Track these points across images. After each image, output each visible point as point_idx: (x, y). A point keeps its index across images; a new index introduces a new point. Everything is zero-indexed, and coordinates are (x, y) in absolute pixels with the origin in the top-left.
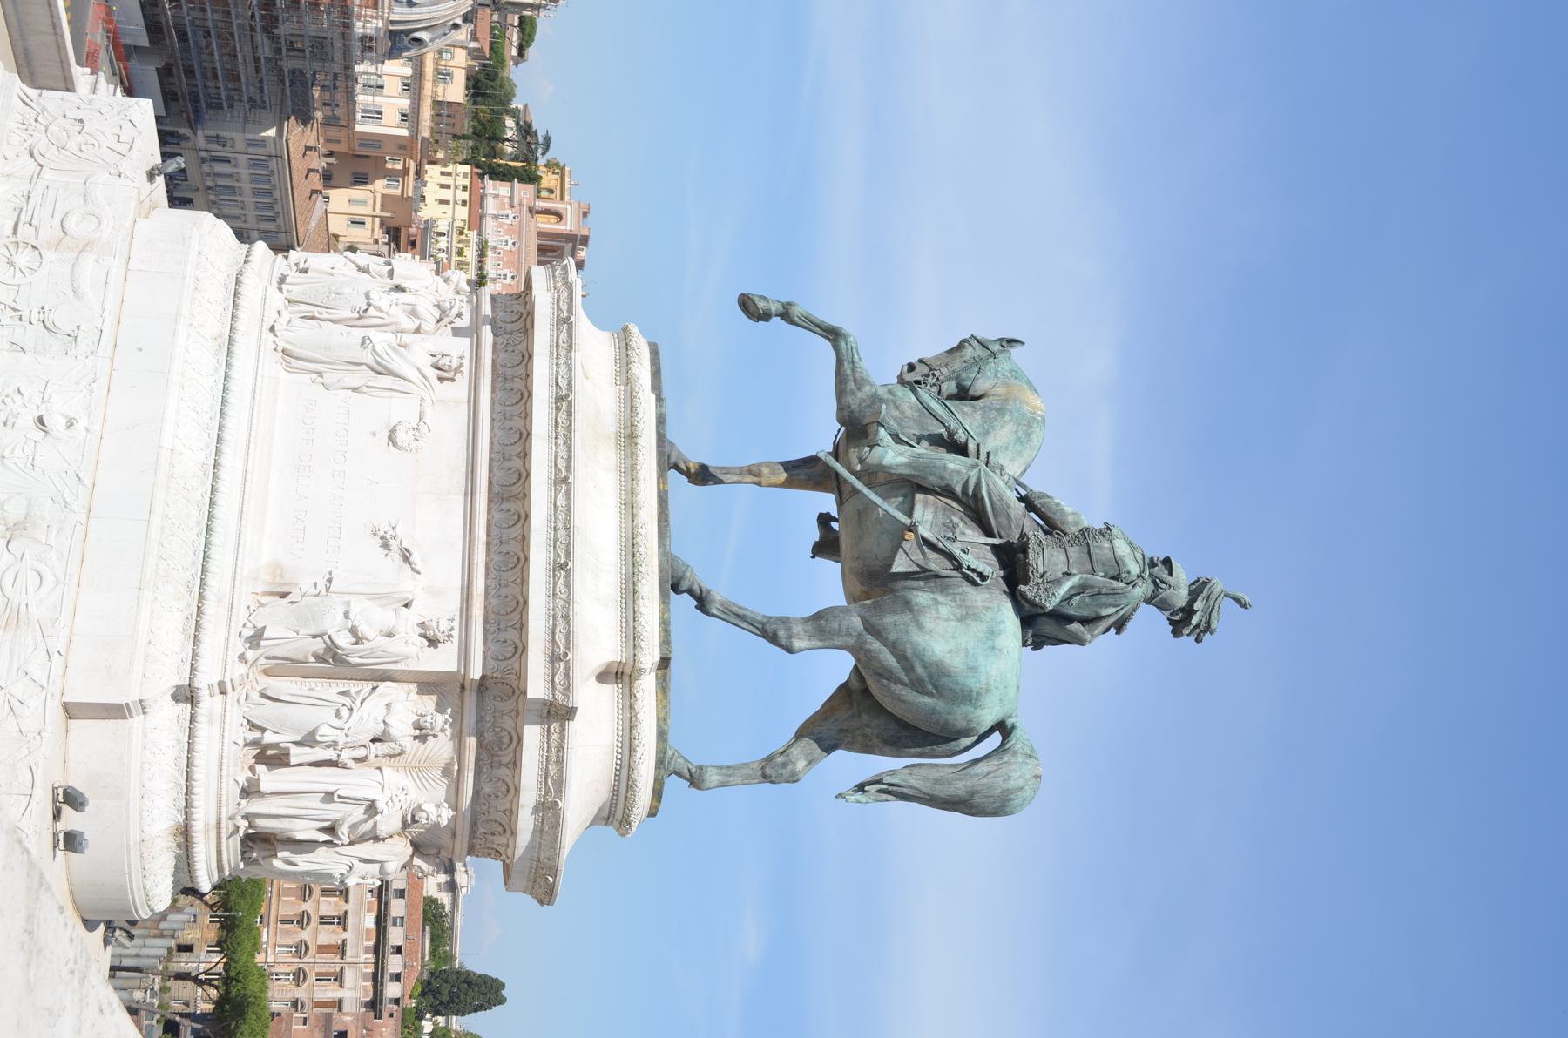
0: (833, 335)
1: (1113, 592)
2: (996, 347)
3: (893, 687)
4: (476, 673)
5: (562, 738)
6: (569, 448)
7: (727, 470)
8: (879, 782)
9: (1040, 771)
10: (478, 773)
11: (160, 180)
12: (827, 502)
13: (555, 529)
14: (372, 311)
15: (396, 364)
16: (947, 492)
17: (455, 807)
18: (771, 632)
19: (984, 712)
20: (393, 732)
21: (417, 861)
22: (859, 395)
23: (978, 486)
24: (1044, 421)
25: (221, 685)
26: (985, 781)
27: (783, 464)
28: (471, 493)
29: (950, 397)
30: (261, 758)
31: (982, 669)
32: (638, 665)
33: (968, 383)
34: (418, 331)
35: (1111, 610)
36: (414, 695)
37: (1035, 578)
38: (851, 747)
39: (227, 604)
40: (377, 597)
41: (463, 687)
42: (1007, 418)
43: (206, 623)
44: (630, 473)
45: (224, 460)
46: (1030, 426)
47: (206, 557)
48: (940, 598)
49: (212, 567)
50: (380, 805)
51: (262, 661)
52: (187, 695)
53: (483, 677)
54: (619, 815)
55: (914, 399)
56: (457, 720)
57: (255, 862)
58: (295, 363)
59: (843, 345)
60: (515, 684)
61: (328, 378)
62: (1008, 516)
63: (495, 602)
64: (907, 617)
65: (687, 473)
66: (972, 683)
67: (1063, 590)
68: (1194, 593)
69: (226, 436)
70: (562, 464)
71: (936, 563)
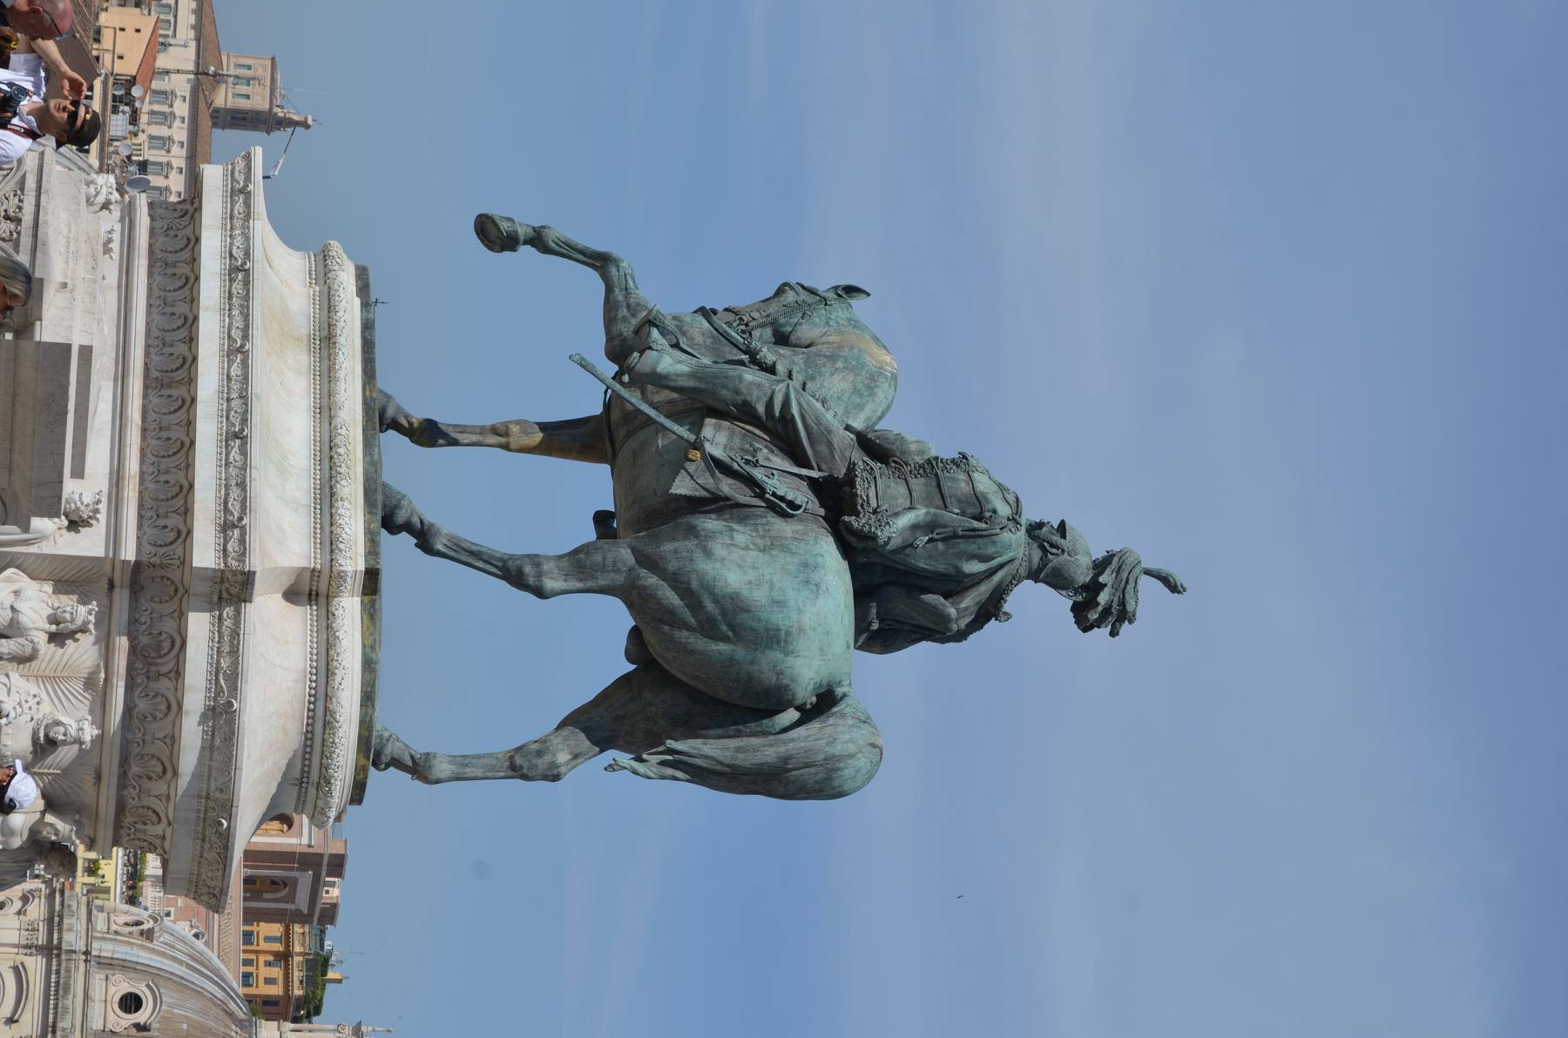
0: (600, 262)
1: (973, 535)
3: (677, 634)
4: (129, 553)
5: (237, 623)
6: (246, 317)
7: (464, 429)
10: (130, 687)
13: (228, 400)
21: (49, 818)
23: (786, 404)
24: (895, 377)
31: (792, 603)
33: (788, 329)
42: (840, 364)
44: (326, 375)
46: (873, 379)
48: (735, 526)
53: (138, 564)
54: (314, 777)
55: (706, 324)
56: (104, 618)
59: (613, 271)
62: (830, 444)
64: (691, 544)
66: (778, 619)
71: (727, 486)
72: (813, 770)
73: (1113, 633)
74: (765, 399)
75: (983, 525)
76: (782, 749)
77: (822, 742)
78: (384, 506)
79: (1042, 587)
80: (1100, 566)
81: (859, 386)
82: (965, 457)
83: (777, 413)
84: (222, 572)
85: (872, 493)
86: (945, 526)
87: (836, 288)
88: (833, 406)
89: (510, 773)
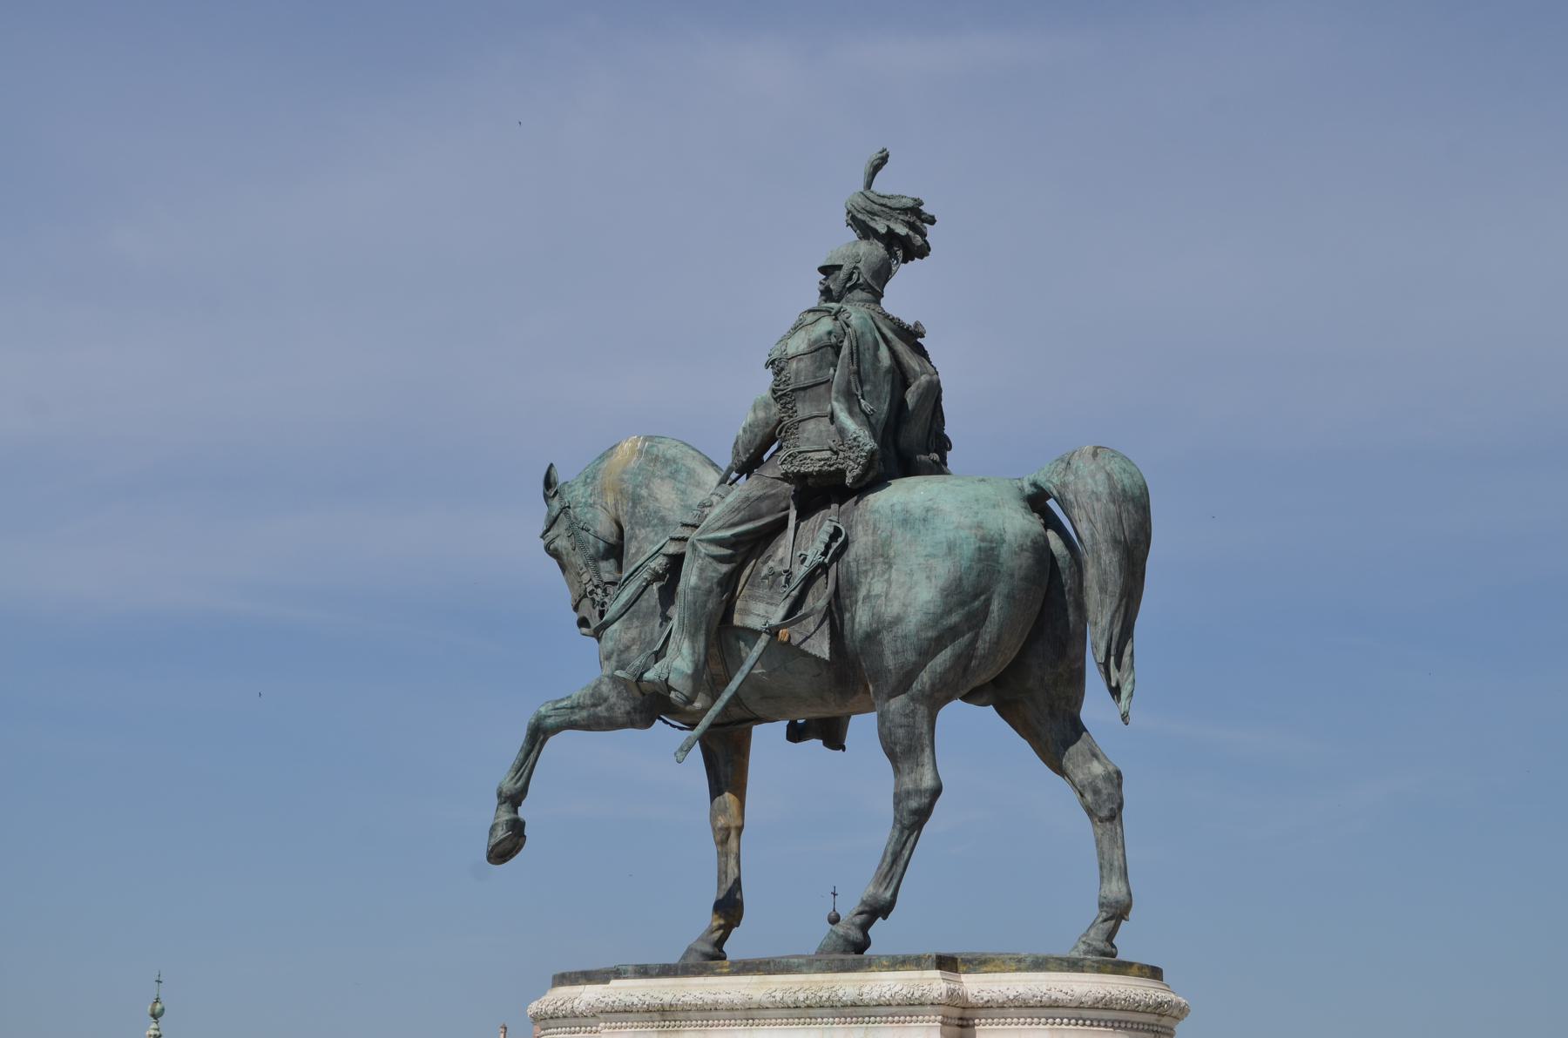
0: (538, 735)
1: (855, 354)
7: (722, 873)
8: (1106, 665)
9: (1088, 448)
12: (767, 739)
16: (728, 586)
18: (914, 817)
19: (1009, 529)
22: (612, 700)
26: (1099, 525)
27: (712, 799)
29: (620, 568)
31: (951, 535)
32: (944, 999)
33: (601, 545)
42: (644, 492)
46: (657, 458)
48: (863, 592)
54: (1152, 1019)
55: (615, 626)
59: (550, 721)
62: (760, 499)
64: (887, 638)
65: (727, 929)
66: (968, 549)
71: (818, 600)
72: (1124, 515)
73: (932, 221)
74: (715, 564)
75: (846, 343)
76: (1103, 547)
77: (1097, 506)
78: (845, 952)
79: (889, 288)
80: (866, 232)
81: (666, 473)
82: (772, 363)
83: (729, 552)
85: (817, 456)
86: (849, 382)
87: (546, 497)
88: (699, 498)
89: (1116, 822)
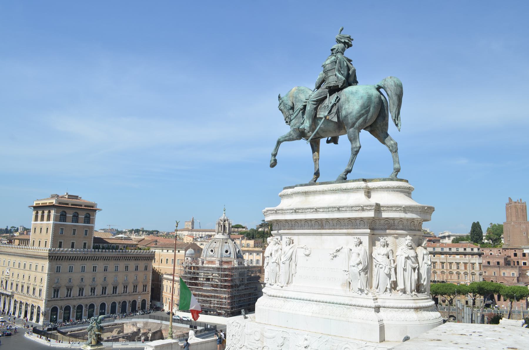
0: (279, 143)
1: (340, 63)
2: (281, 101)
4: (368, 231)
5: (385, 207)
6: (308, 209)
7: (315, 168)
8: (395, 120)
9: (389, 77)
11: (247, 315)
14: (277, 261)
15: (289, 255)
16: (316, 109)
17: (407, 235)
18: (356, 152)
20: (386, 253)
21: (423, 245)
23: (314, 101)
25: (374, 300)
28: (321, 234)
30: (395, 288)
34: (281, 249)
35: (345, 63)
36: (376, 248)
37: (337, 84)
38: (387, 129)
39: (352, 298)
40: (349, 258)
41: (373, 234)
43: (357, 304)
44: (315, 193)
45: (315, 299)
47: (340, 304)
49: (342, 302)
50: (406, 256)
51: (367, 289)
52: (377, 309)
54: (408, 190)
56: (383, 235)
57: (425, 289)
58: (290, 281)
60: (371, 220)
61: (293, 272)
63: (349, 227)
64: (349, 116)
65: (317, 178)
66: (366, 97)
67: (340, 76)
68: (340, 42)
69: (309, 299)
70: (312, 210)
71: (334, 110)
76: (393, 96)
84: (375, 210)
